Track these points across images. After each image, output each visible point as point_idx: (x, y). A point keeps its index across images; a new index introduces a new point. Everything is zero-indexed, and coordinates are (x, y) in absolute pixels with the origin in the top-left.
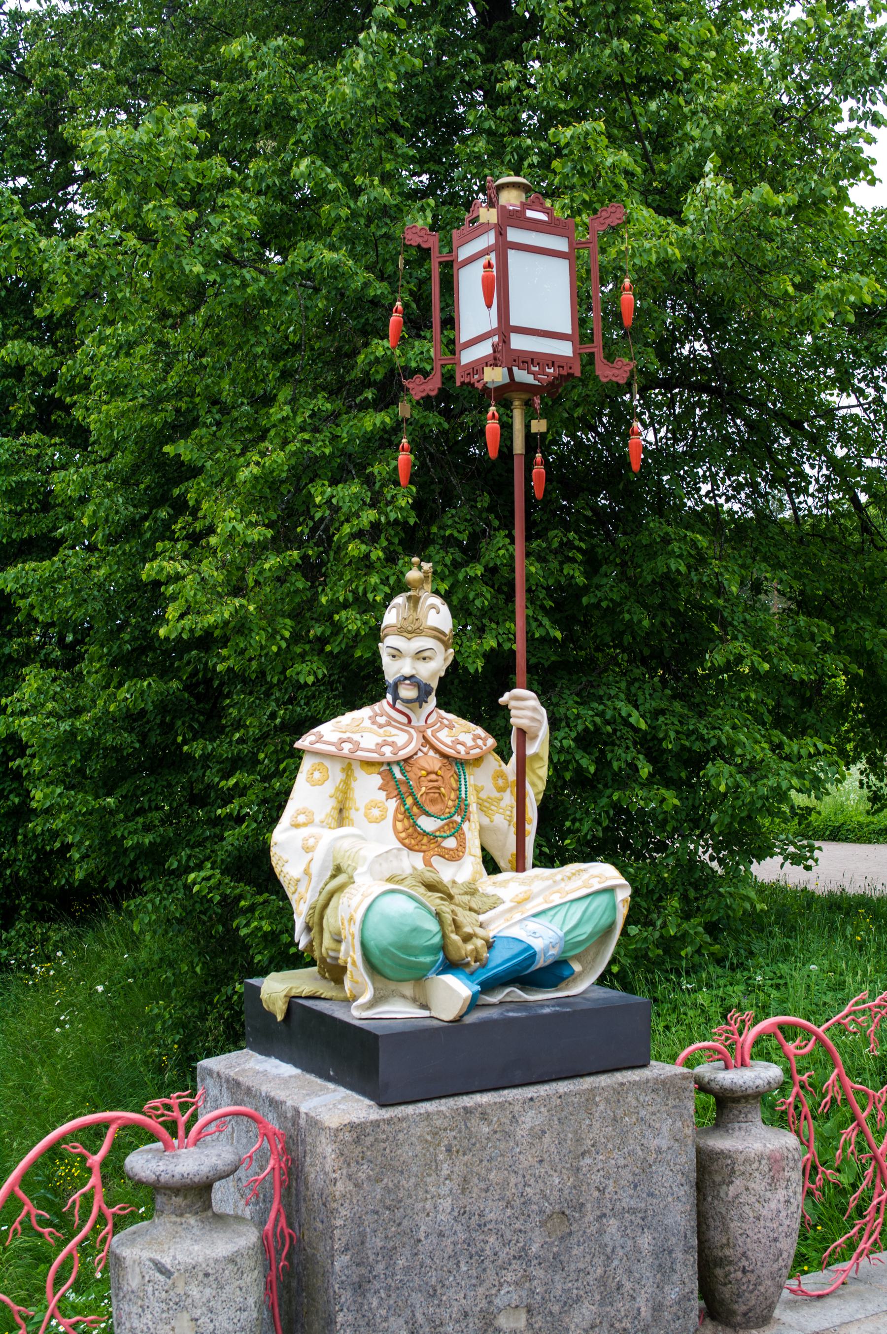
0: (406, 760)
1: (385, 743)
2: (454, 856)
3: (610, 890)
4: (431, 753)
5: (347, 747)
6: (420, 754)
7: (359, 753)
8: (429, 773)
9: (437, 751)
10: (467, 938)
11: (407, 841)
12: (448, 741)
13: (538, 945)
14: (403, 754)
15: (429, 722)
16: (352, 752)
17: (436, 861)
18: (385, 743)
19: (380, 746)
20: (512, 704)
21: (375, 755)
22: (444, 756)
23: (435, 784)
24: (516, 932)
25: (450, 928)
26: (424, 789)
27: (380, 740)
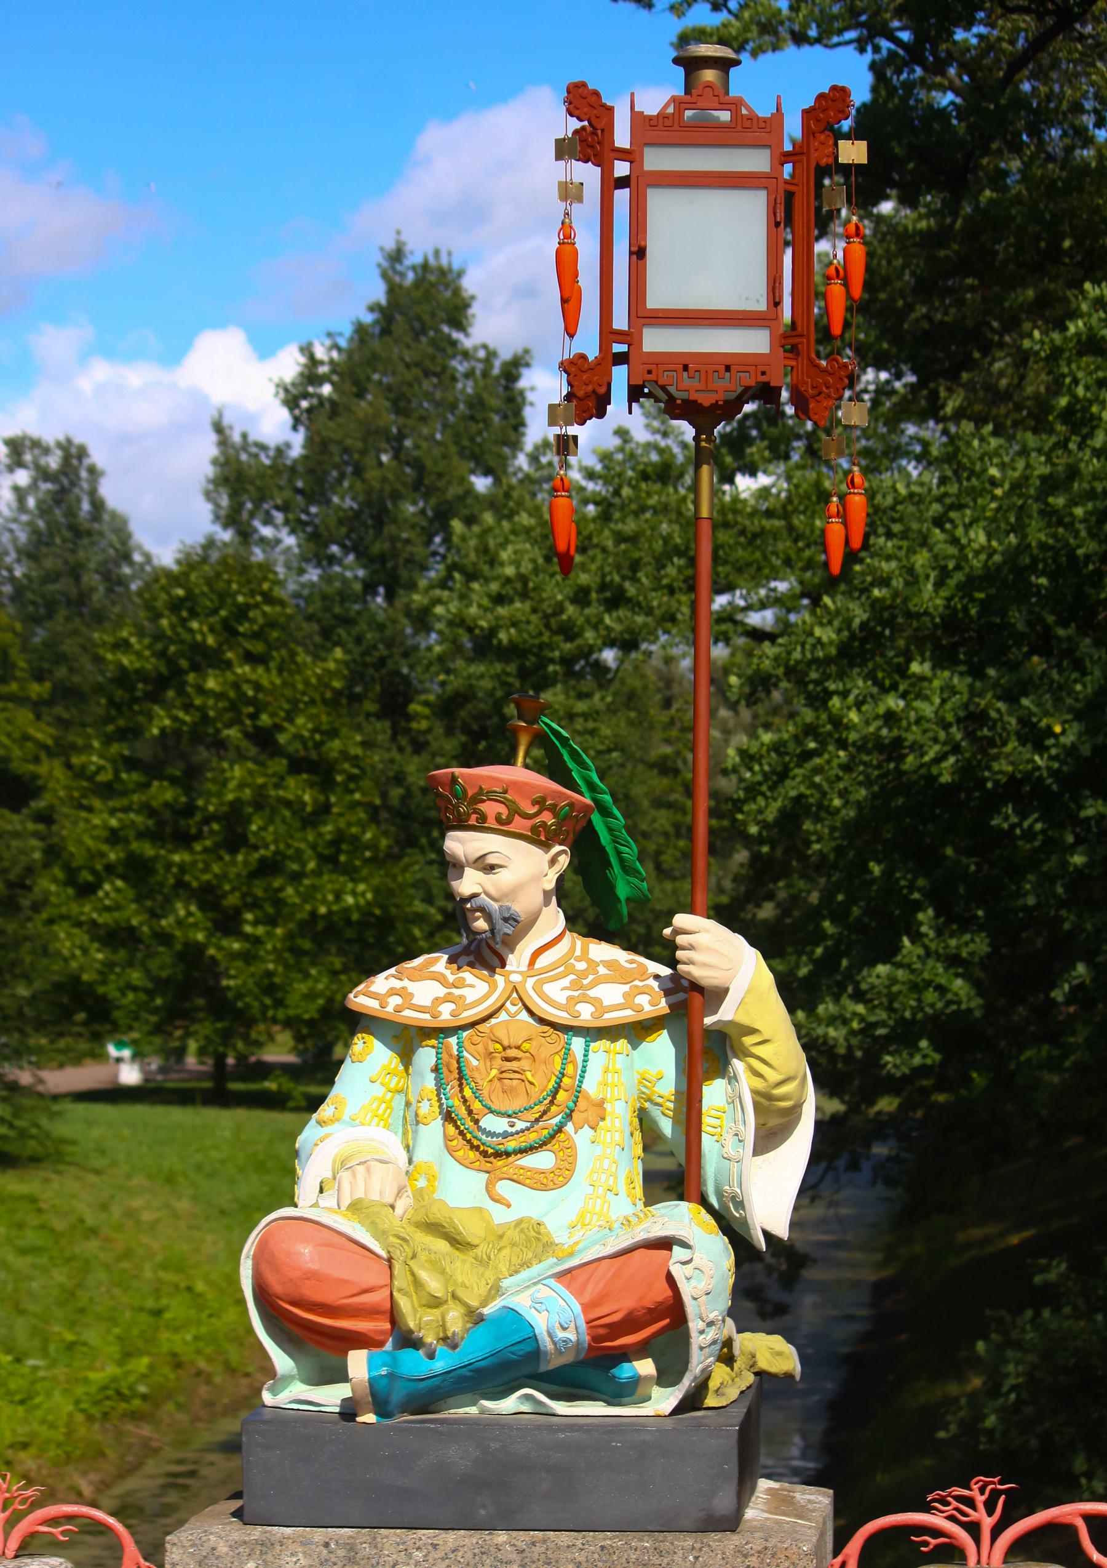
0: (473, 1025)
1: (448, 999)
2: (542, 1182)
3: (665, 1244)
4: (524, 1016)
5: (394, 1001)
6: (503, 1016)
7: (407, 1013)
8: (504, 1049)
9: (531, 1013)
10: (435, 1303)
11: (461, 1153)
12: (561, 997)
13: (540, 1323)
14: (468, 1015)
15: (538, 965)
16: (398, 1010)
17: (504, 1188)
18: (448, 999)
19: (438, 1001)
20: (681, 940)
21: (427, 1016)
22: (542, 1021)
23: (514, 1065)
24: (521, 1302)
25: (401, 1280)
26: (494, 1072)
27: (441, 991)
